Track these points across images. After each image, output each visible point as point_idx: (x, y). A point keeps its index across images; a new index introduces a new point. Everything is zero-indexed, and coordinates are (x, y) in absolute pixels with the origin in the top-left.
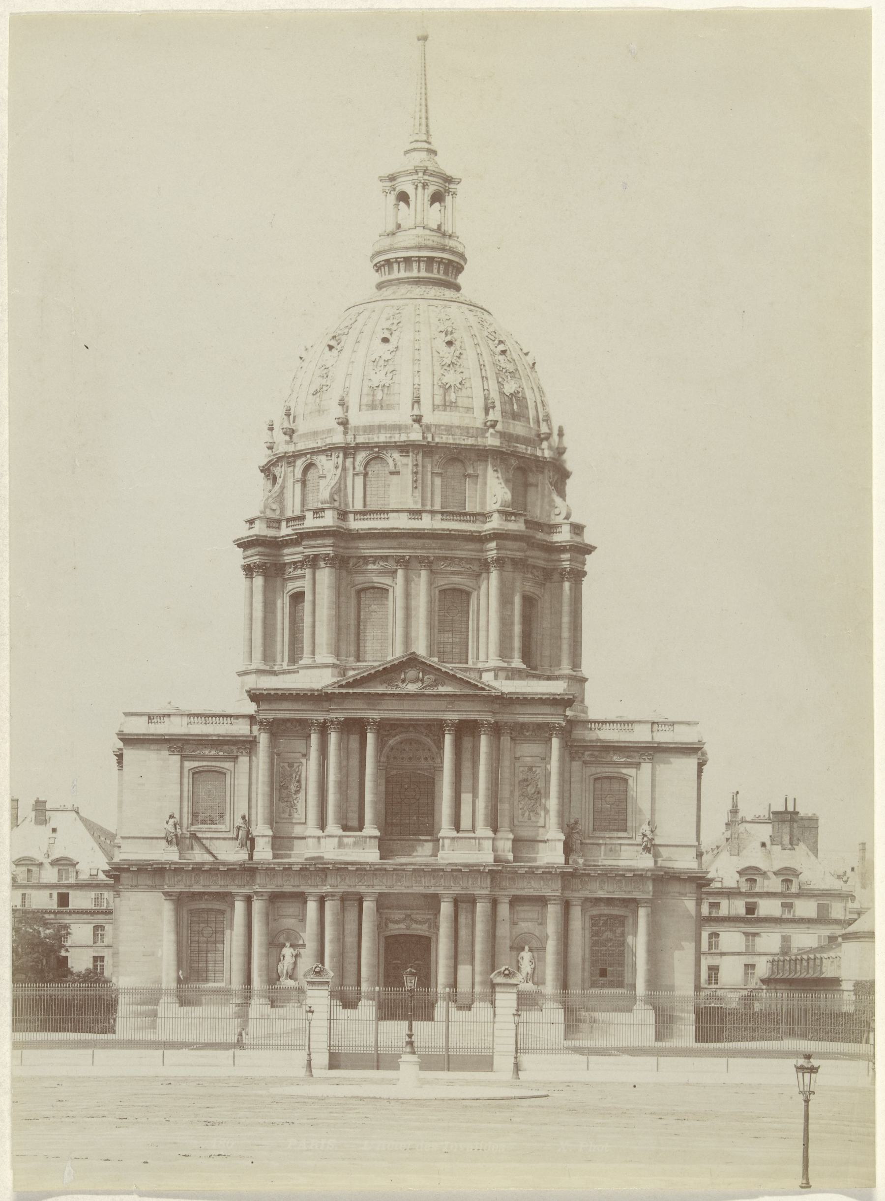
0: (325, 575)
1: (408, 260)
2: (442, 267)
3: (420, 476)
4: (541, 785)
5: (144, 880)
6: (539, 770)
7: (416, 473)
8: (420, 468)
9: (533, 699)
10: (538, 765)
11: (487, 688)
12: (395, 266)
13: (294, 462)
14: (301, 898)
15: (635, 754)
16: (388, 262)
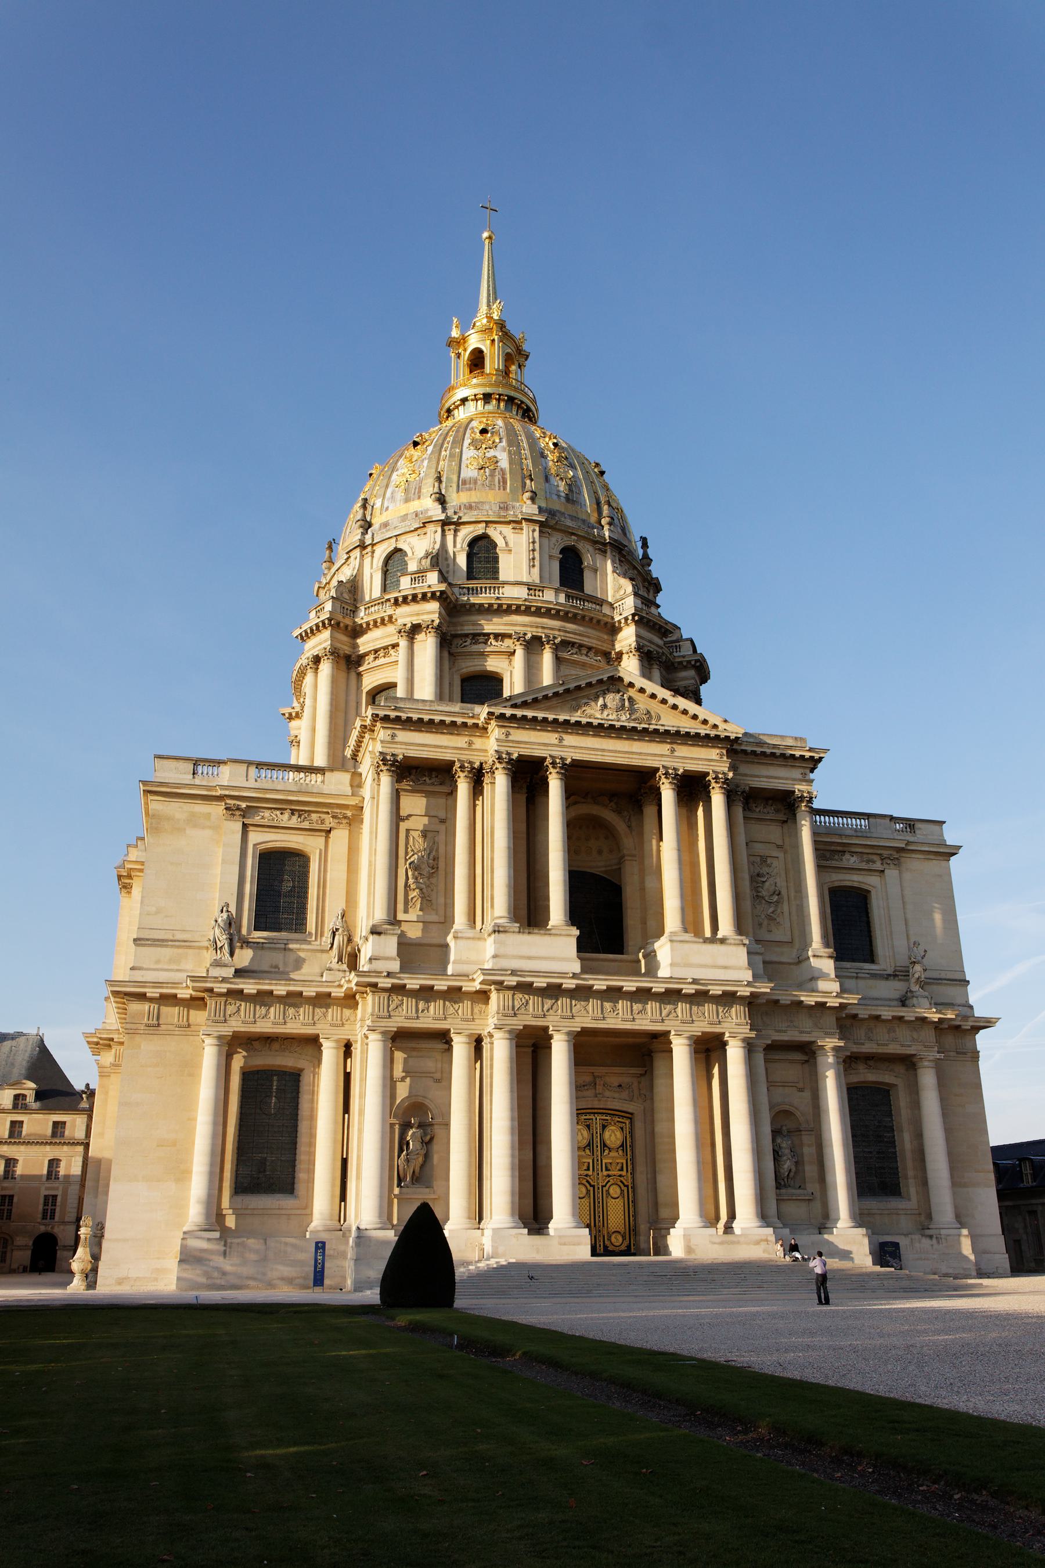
0: (427, 646)
1: (487, 398)
2: (520, 412)
3: (537, 554)
4: (781, 883)
5: (171, 1014)
6: (775, 863)
7: (533, 550)
8: (537, 546)
9: (773, 754)
10: (774, 854)
11: (722, 726)
12: (471, 405)
13: (373, 552)
14: (443, 1037)
15: (875, 858)
16: (464, 401)
